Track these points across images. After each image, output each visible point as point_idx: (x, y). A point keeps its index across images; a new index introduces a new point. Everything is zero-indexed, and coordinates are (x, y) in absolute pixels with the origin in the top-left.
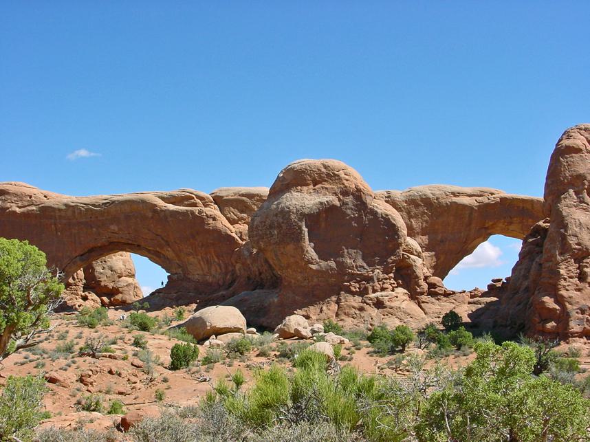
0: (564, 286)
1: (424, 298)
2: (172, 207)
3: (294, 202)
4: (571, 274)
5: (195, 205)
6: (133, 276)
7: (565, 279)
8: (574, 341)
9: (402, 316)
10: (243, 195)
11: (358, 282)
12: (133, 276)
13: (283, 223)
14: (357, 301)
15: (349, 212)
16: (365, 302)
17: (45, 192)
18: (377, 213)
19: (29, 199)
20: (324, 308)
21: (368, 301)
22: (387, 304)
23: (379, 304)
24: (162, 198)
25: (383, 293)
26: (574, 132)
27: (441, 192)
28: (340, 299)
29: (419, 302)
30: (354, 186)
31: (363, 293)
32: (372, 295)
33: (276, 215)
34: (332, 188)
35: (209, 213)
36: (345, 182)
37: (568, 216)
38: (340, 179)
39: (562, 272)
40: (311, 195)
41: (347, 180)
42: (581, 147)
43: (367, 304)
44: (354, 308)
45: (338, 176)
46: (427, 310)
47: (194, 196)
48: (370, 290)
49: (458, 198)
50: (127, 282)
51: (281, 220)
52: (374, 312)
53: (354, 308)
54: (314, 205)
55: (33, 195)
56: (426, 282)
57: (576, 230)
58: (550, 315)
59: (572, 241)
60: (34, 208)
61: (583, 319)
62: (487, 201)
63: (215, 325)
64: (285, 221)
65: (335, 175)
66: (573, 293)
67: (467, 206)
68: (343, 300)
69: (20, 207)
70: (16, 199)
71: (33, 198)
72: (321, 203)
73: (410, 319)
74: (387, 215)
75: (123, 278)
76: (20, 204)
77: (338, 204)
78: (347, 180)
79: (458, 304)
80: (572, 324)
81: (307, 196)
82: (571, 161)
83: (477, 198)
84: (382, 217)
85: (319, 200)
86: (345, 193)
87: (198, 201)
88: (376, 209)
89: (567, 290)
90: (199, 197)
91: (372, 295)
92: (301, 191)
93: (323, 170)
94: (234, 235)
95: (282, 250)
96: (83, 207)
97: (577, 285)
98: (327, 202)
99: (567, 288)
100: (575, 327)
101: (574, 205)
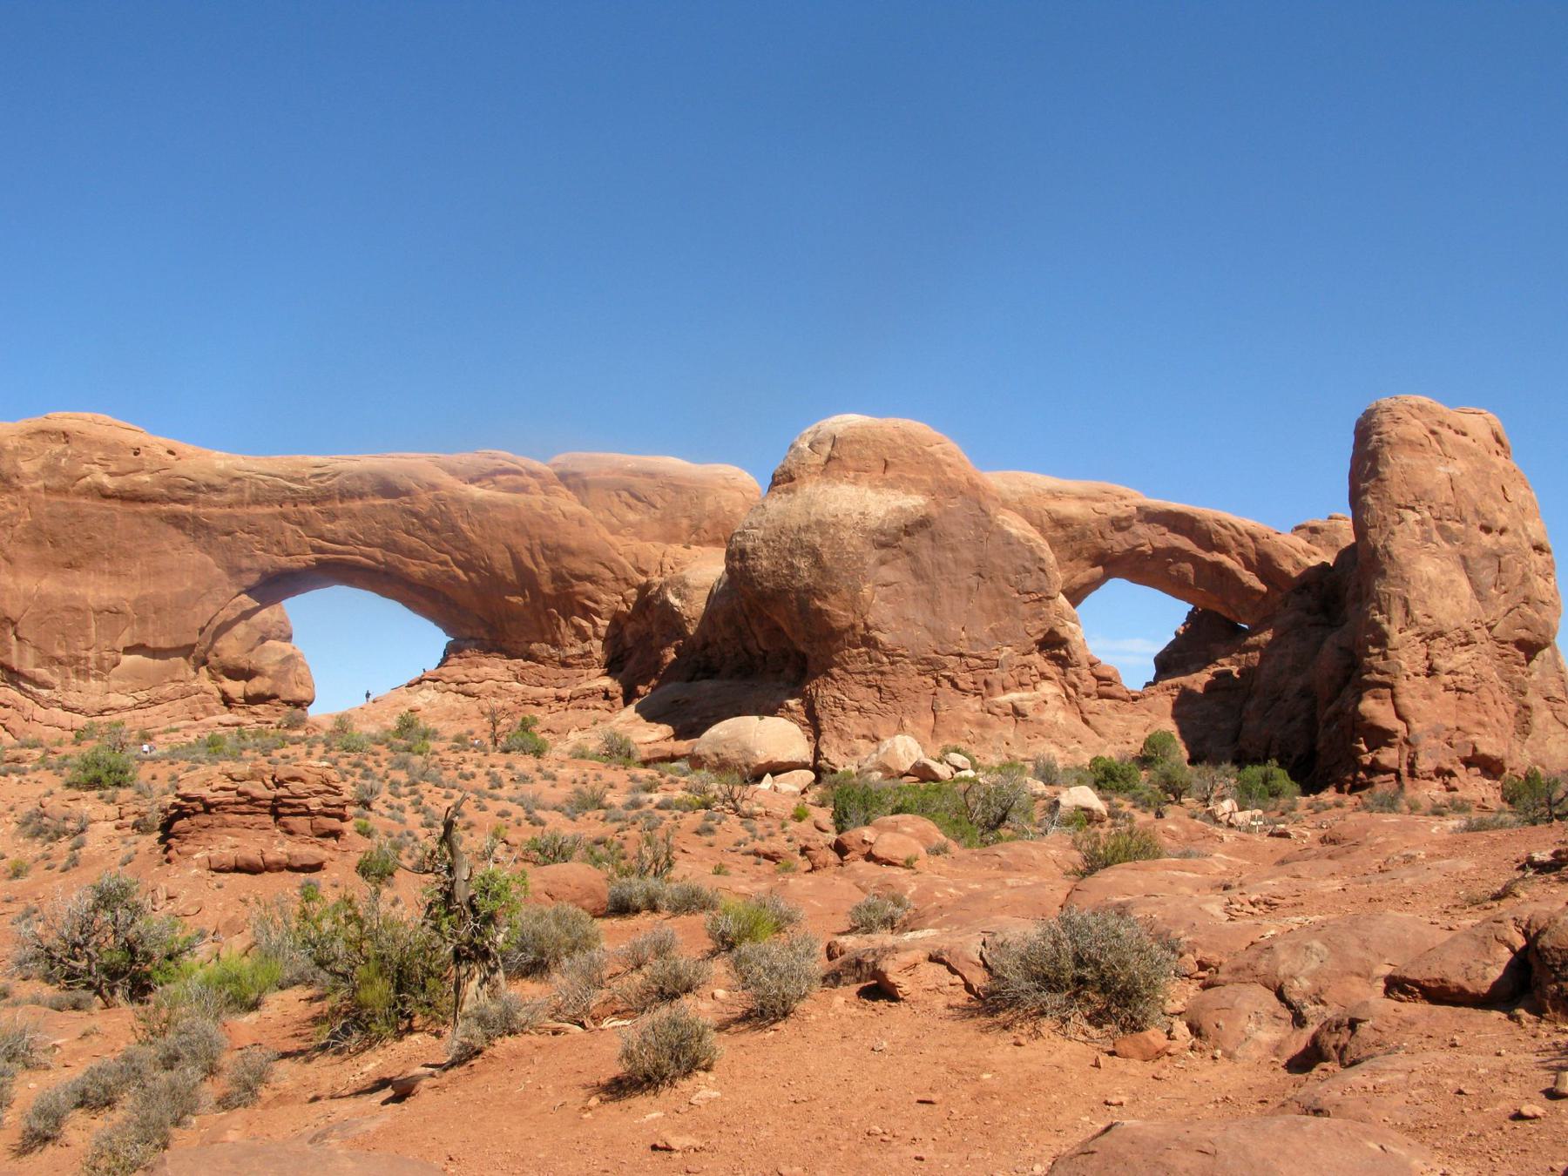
0: (1408, 690)
1: (1092, 704)
2: (477, 492)
3: (845, 505)
4: (1419, 669)
5: (522, 489)
6: (289, 638)
7: (1408, 677)
8: (1425, 786)
9: (1063, 739)
10: (634, 473)
11: (971, 669)
12: (289, 638)
13: (821, 545)
14: (973, 710)
15: (954, 529)
16: (989, 712)
17: (174, 444)
18: (1010, 535)
19: (132, 456)
20: (907, 722)
21: (997, 711)
22: (1031, 715)
23: (1017, 713)
24: (453, 472)
25: (1025, 695)
26: (1401, 411)
27: (1027, 489)
28: (939, 705)
29: (1081, 712)
30: (963, 479)
31: (983, 689)
32: (1004, 699)
33: (808, 528)
34: (921, 481)
35: (566, 508)
36: (948, 469)
37: (1409, 565)
38: (937, 463)
39: (1404, 664)
40: (879, 493)
41: (950, 466)
42: (1425, 442)
43: (993, 714)
44: (968, 722)
45: (932, 455)
46: (1102, 729)
47: (523, 470)
48: (997, 688)
49: (1060, 503)
50: (283, 651)
51: (818, 540)
52: (1009, 730)
53: (968, 722)
54: (888, 512)
55: (142, 448)
56: (1093, 675)
57: (1425, 590)
58: (1381, 737)
59: (1417, 612)
60: (146, 478)
61: (1437, 748)
62: (1113, 512)
63: (775, 755)
64: (828, 543)
65: (924, 452)
66: (1423, 704)
67: (1078, 519)
68: (945, 707)
69: (111, 474)
70: (100, 454)
71: (142, 455)
72: (901, 510)
73: (1077, 746)
74: (1029, 540)
75: (270, 643)
76: (113, 468)
77: (934, 511)
78: (950, 466)
79: (1155, 717)
80: (1421, 756)
81: (870, 494)
82: (1408, 465)
83: (1097, 506)
84: (1019, 543)
85: (899, 503)
86: (952, 490)
87: (531, 480)
88: (1007, 528)
89: (1412, 697)
90: (532, 474)
91: (1004, 699)
92: (855, 482)
93: (900, 441)
94: (622, 559)
95: (818, 603)
96: (263, 481)
97: (1427, 689)
98: (915, 507)
99: (1412, 692)
100: (1425, 764)
101: (1417, 546)
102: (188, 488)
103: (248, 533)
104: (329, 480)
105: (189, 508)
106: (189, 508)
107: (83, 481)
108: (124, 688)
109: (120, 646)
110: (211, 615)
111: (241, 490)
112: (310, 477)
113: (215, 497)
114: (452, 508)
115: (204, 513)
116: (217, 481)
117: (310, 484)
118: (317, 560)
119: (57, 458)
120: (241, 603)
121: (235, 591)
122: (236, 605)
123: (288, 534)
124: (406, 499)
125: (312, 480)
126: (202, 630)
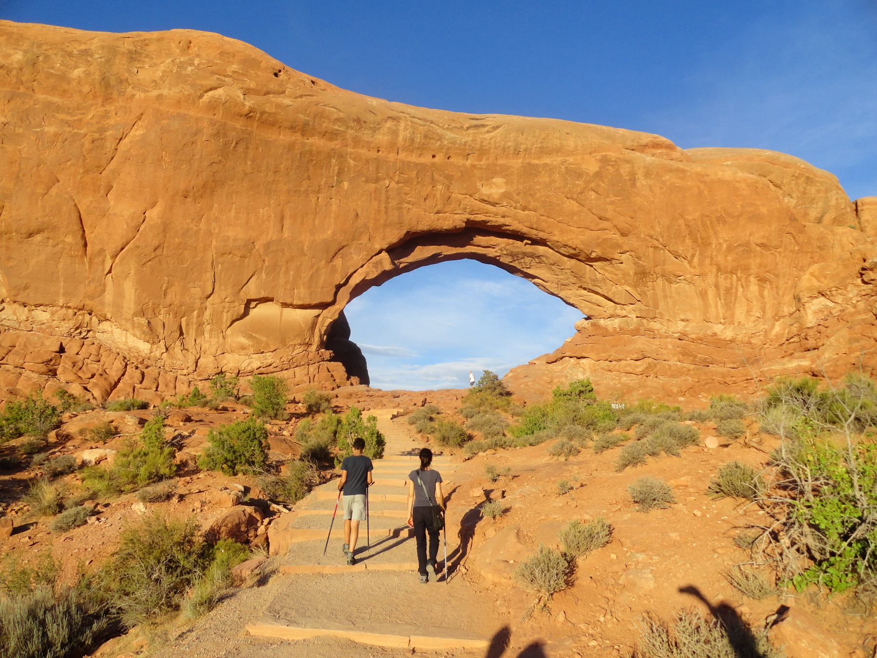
102: (338, 120)
103: (398, 183)
104: (488, 132)
105: (335, 144)
106: (335, 144)
107: (210, 93)
108: (243, 348)
109: (244, 296)
110: (351, 271)
111: (395, 133)
112: (468, 128)
113: (366, 135)
114: (622, 171)
115: (351, 153)
116: (370, 118)
117: (469, 135)
118: (468, 222)
119: (181, 66)
120: (380, 262)
121: (378, 247)
122: (377, 263)
123: (440, 187)
124: (571, 159)
125: (471, 131)
126: (339, 287)
